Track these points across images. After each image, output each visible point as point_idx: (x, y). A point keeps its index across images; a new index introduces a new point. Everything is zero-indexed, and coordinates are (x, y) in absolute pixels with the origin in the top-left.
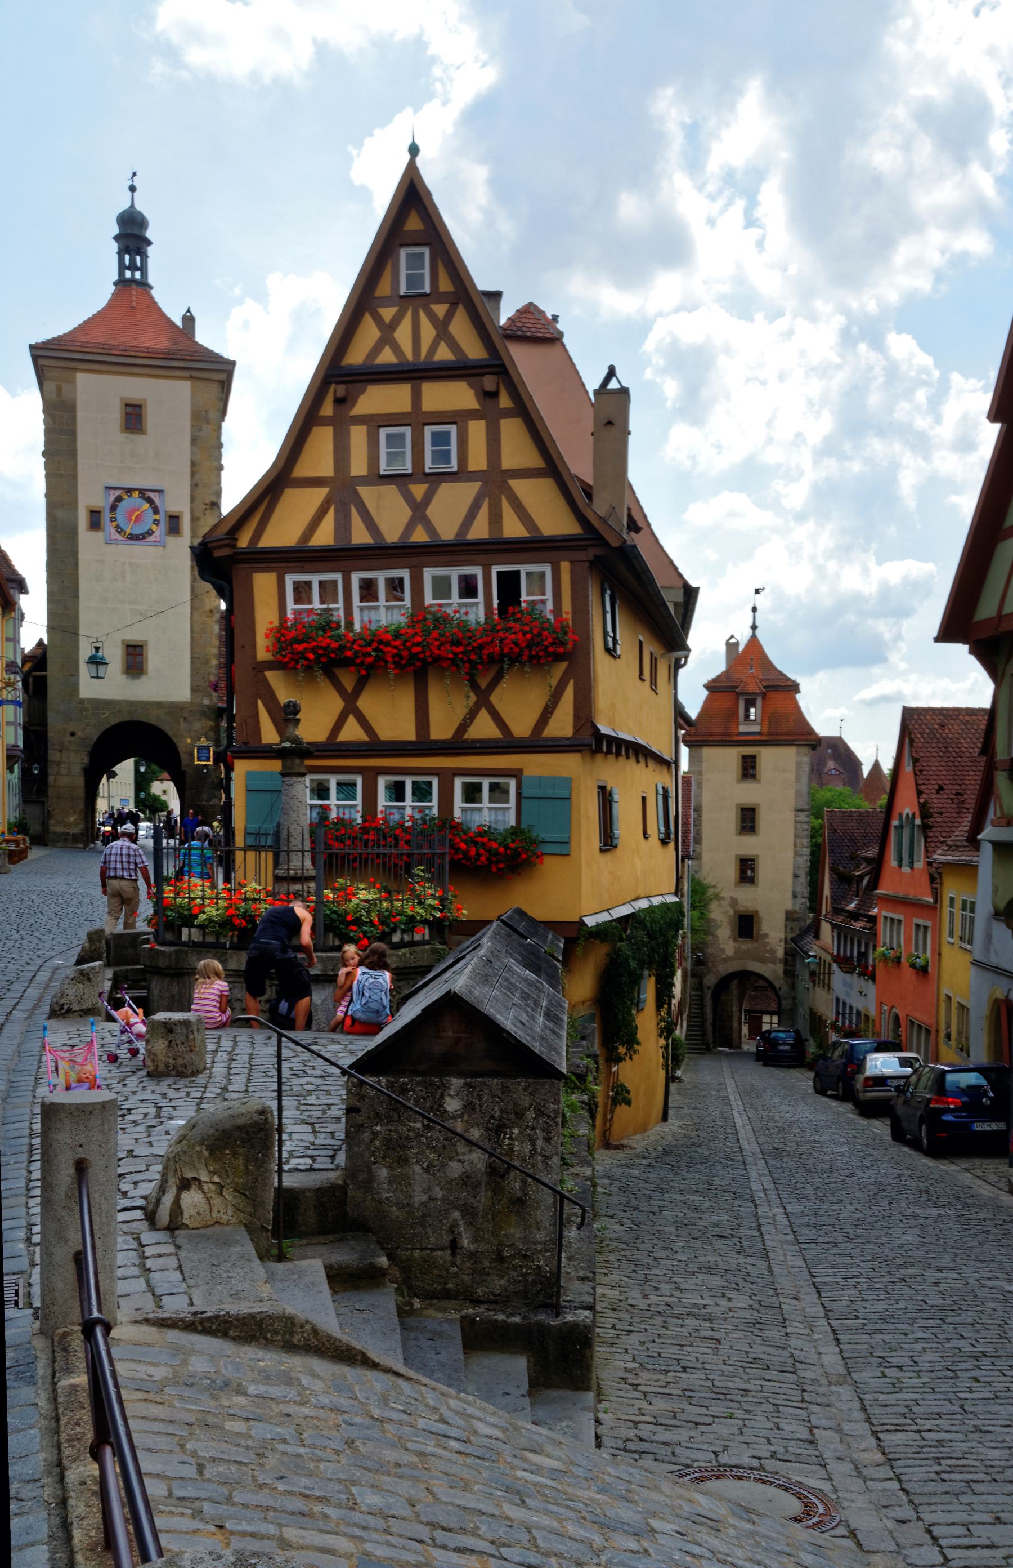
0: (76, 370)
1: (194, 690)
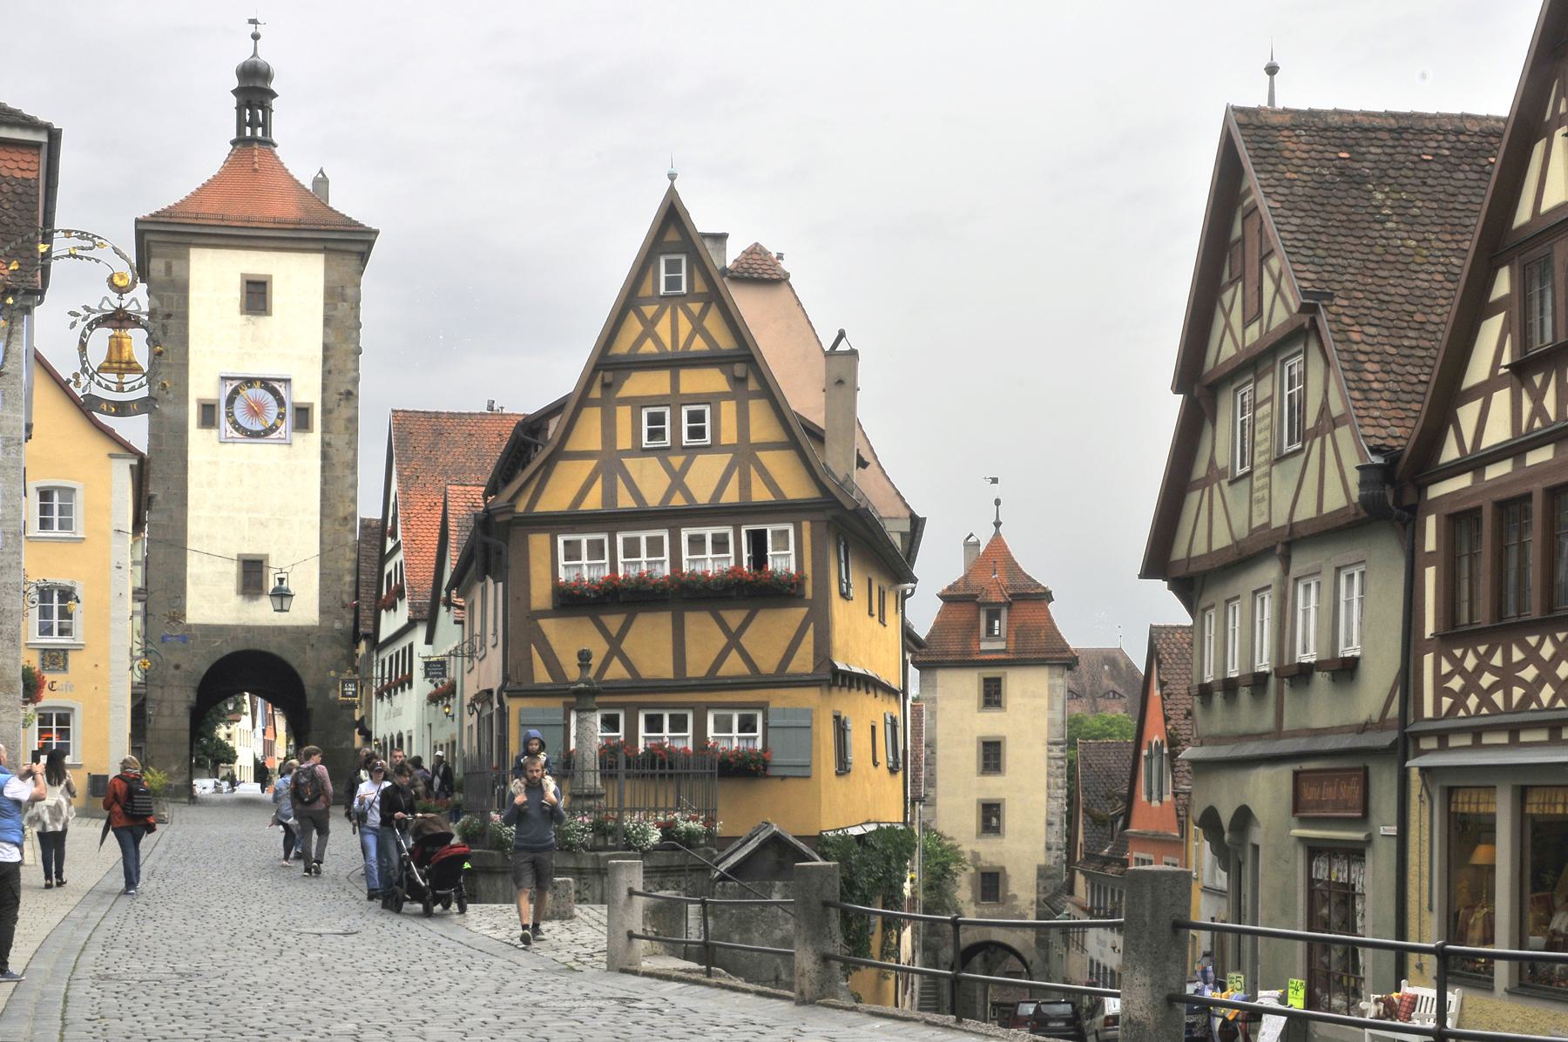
1: (322, 612)
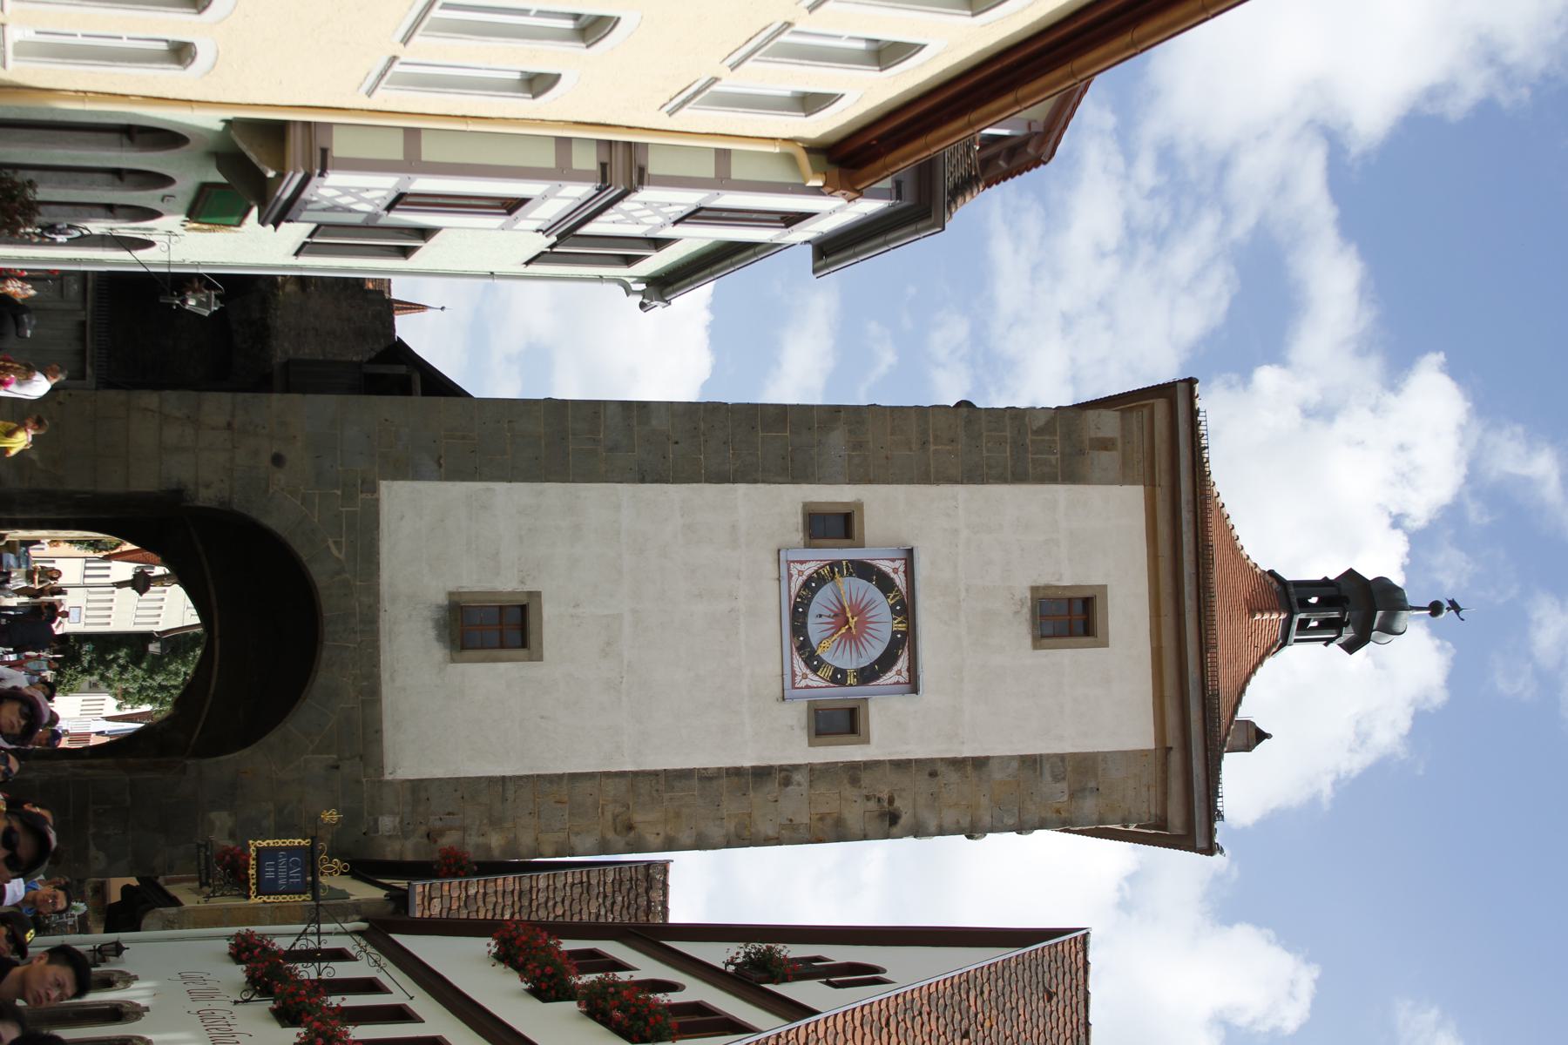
0: (1151, 485)
1: (418, 788)
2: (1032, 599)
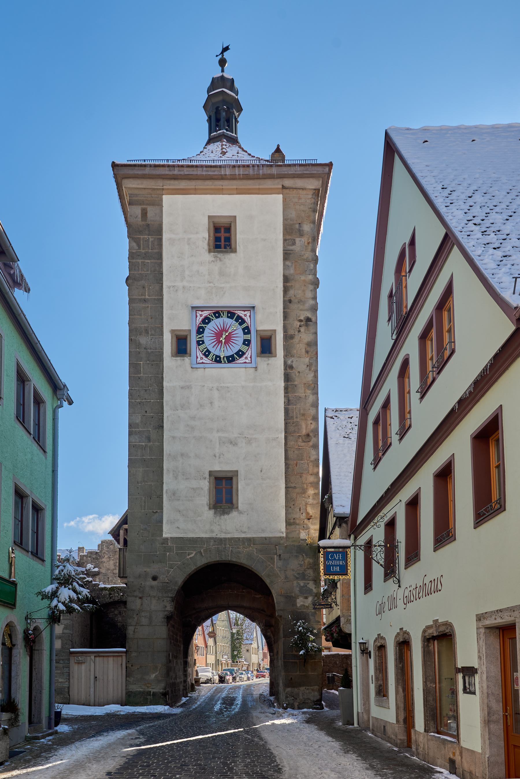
0: (162, 191)
2: (214, 252)
